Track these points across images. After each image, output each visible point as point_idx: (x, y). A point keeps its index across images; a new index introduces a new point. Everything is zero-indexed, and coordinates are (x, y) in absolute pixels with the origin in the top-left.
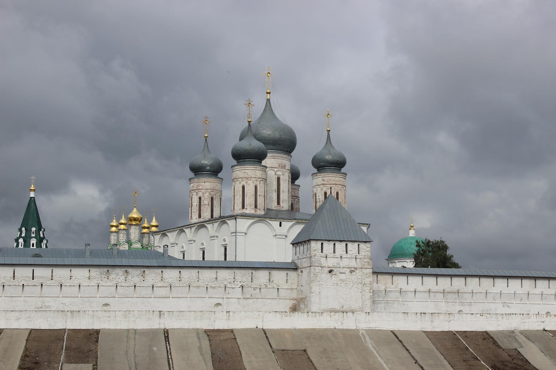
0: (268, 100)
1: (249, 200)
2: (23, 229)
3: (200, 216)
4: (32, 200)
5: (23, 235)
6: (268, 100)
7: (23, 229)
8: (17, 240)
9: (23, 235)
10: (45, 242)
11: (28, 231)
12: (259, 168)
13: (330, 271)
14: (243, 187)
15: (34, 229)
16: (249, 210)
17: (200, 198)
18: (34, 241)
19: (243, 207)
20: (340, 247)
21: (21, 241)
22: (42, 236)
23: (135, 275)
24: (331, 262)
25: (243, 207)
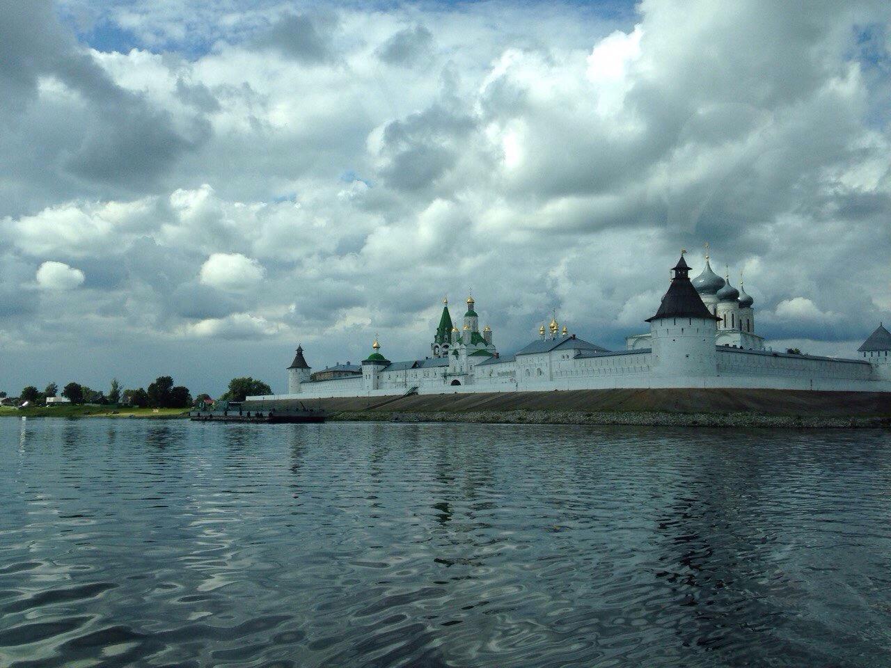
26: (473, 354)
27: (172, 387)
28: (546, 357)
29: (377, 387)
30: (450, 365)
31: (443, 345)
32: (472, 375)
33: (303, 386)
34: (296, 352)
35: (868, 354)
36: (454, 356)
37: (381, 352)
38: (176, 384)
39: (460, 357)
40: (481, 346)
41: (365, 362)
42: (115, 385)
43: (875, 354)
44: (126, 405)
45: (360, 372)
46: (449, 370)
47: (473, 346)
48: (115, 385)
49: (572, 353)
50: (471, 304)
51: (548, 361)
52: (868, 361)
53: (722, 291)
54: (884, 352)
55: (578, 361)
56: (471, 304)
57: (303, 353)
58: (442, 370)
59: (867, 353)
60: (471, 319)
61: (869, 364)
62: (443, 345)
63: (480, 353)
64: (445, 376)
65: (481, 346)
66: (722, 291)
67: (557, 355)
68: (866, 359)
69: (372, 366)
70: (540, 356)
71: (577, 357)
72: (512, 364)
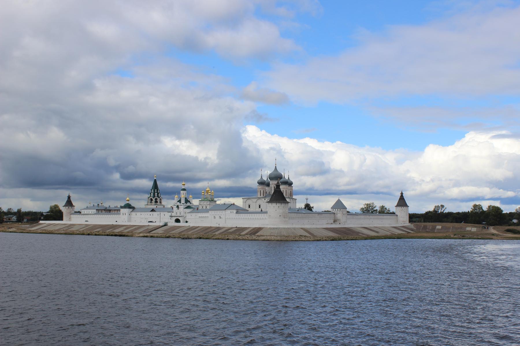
0: (276, 166)
2: (153, 190)
3: (263, 195)
4: (155, 180)
5: (153, 192)
6: (276, 166)
7: (153, 190)
8: (150, 194)
9: (153, 192)
10: (160, 194)
11: (154, 191)
14: (286, 191)
15: (156, 190)
17: (263, 191)
18: (156, 194)
21: (152, 194)
22: (159, 192)
26: (186, 208)
28: (224, 212)
29: (129, 220)
31: (155, 198)
33: (72, 216)
34: (67, 198)
35: (334, 209)
36: (177, 208)
39: (179, 209)
40: (188, 204)
43: (337, 210)
46: (173, 214)
47: (185, 204)
49: (235, 211)
51: (224, 214)
52: (334, 212)
53: (282, 180)
54: (339, 209)
55: (237, 214)
57: (71, 198)
58: (170, 214)
61: (334, 214)
63: (188, 207)
64: (171, 216)
65: (188, 204)
66: (282, 180)
67: (228, 212)
68: (334, 212)
69: (127, 209)
70: (221, 211)
71: (237, 213)
72: (208, 213)
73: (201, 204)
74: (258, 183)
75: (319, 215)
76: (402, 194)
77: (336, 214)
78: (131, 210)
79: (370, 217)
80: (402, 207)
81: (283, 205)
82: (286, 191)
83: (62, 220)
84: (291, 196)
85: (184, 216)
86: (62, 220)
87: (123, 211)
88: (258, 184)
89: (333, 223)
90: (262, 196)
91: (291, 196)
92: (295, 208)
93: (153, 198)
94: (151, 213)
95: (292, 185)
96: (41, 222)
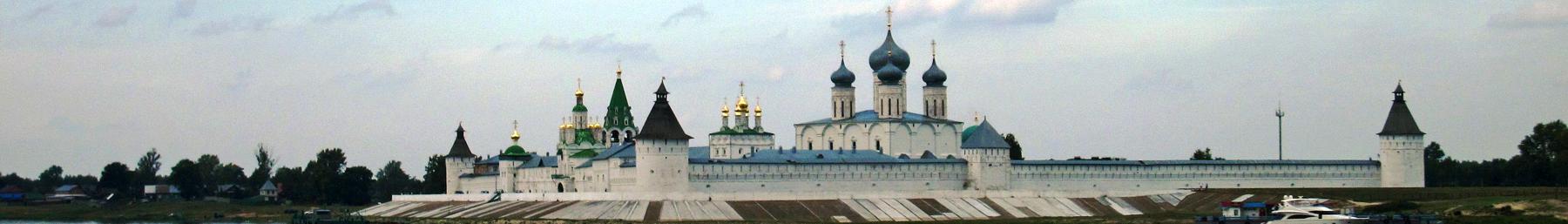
1: (894, 109)
3: (843, 115)
12: (895, 87)
13: (990, 165)
14: (890, 100)
16: (894, 116)
17: (843, 102)
19: (890, 114)
20: (995, 151)
23: (887, 169)
24: (991, 160)
25: (890, 114)
27: (343, 170)
28: (605, 163)
30: (559, 165)
31: (612, 130)
32: (573, 179)
34: (456, 134)
37: (520, 143)
38: (351, 162)
41: (503, 157)
42: (263, 158)
44: (271, 198)
45: (496, 165)
48: (263, 158)
49: (619, 162)
50: (580, 97)
56: (580, 97)
58: (552, 171)
59: (967, 151)
60: (579, 115)
62: (612, 130)
71: (622, 166)
73: (714, 142)
74: (833, 80)
75: (883, 167)
76: (1399, 92)
77: (969, 165)
78: (518, 163)
79: (1224, 172)
80: (1391, 138)
81: (681, 145)
82: (890, 100)
83: (443, 190)
84: (935, 115)
85: (571, 177)
86: (443, 190)
87: (504, 165)
88: (833, 85)
89: (962, 185)
90: (839, 117)
91: (935, 115)
92: (866, 148)
93: (619, 130)
94: (540, 170)
95: (945, 84)
96: (395, 197)
